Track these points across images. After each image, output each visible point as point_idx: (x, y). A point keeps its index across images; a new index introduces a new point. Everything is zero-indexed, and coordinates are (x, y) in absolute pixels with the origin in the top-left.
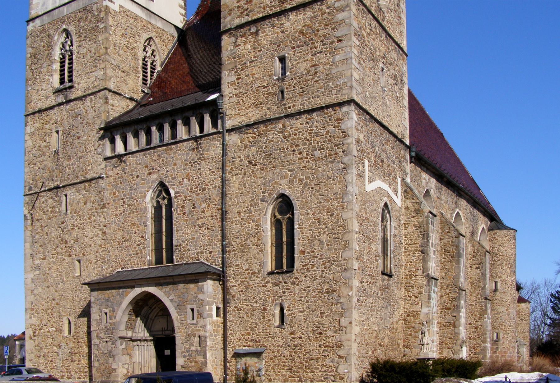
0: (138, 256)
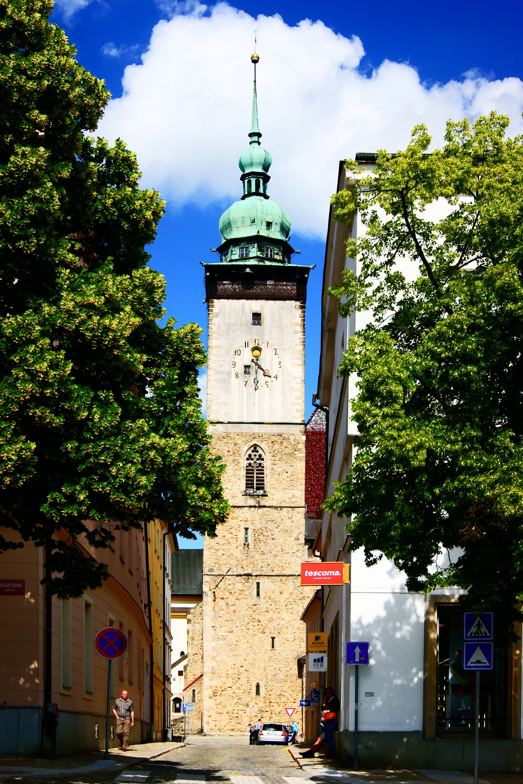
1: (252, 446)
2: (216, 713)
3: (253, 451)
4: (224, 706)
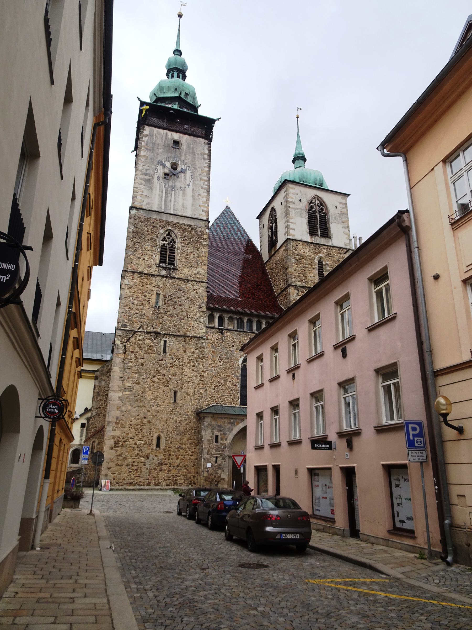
0: (232, 397)
1: (167, 230)
2: (117, 465)
3: (167, 235)
4: (125, 458)
